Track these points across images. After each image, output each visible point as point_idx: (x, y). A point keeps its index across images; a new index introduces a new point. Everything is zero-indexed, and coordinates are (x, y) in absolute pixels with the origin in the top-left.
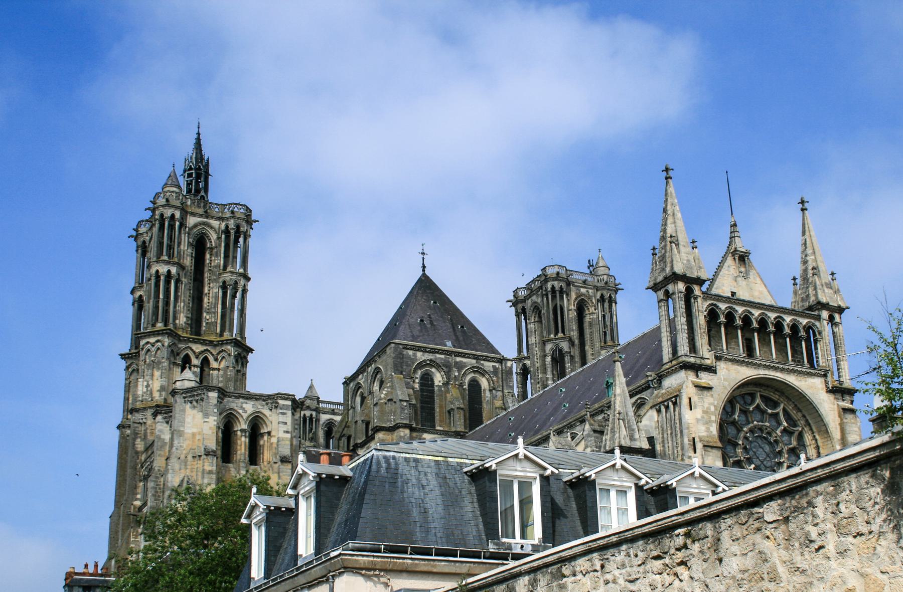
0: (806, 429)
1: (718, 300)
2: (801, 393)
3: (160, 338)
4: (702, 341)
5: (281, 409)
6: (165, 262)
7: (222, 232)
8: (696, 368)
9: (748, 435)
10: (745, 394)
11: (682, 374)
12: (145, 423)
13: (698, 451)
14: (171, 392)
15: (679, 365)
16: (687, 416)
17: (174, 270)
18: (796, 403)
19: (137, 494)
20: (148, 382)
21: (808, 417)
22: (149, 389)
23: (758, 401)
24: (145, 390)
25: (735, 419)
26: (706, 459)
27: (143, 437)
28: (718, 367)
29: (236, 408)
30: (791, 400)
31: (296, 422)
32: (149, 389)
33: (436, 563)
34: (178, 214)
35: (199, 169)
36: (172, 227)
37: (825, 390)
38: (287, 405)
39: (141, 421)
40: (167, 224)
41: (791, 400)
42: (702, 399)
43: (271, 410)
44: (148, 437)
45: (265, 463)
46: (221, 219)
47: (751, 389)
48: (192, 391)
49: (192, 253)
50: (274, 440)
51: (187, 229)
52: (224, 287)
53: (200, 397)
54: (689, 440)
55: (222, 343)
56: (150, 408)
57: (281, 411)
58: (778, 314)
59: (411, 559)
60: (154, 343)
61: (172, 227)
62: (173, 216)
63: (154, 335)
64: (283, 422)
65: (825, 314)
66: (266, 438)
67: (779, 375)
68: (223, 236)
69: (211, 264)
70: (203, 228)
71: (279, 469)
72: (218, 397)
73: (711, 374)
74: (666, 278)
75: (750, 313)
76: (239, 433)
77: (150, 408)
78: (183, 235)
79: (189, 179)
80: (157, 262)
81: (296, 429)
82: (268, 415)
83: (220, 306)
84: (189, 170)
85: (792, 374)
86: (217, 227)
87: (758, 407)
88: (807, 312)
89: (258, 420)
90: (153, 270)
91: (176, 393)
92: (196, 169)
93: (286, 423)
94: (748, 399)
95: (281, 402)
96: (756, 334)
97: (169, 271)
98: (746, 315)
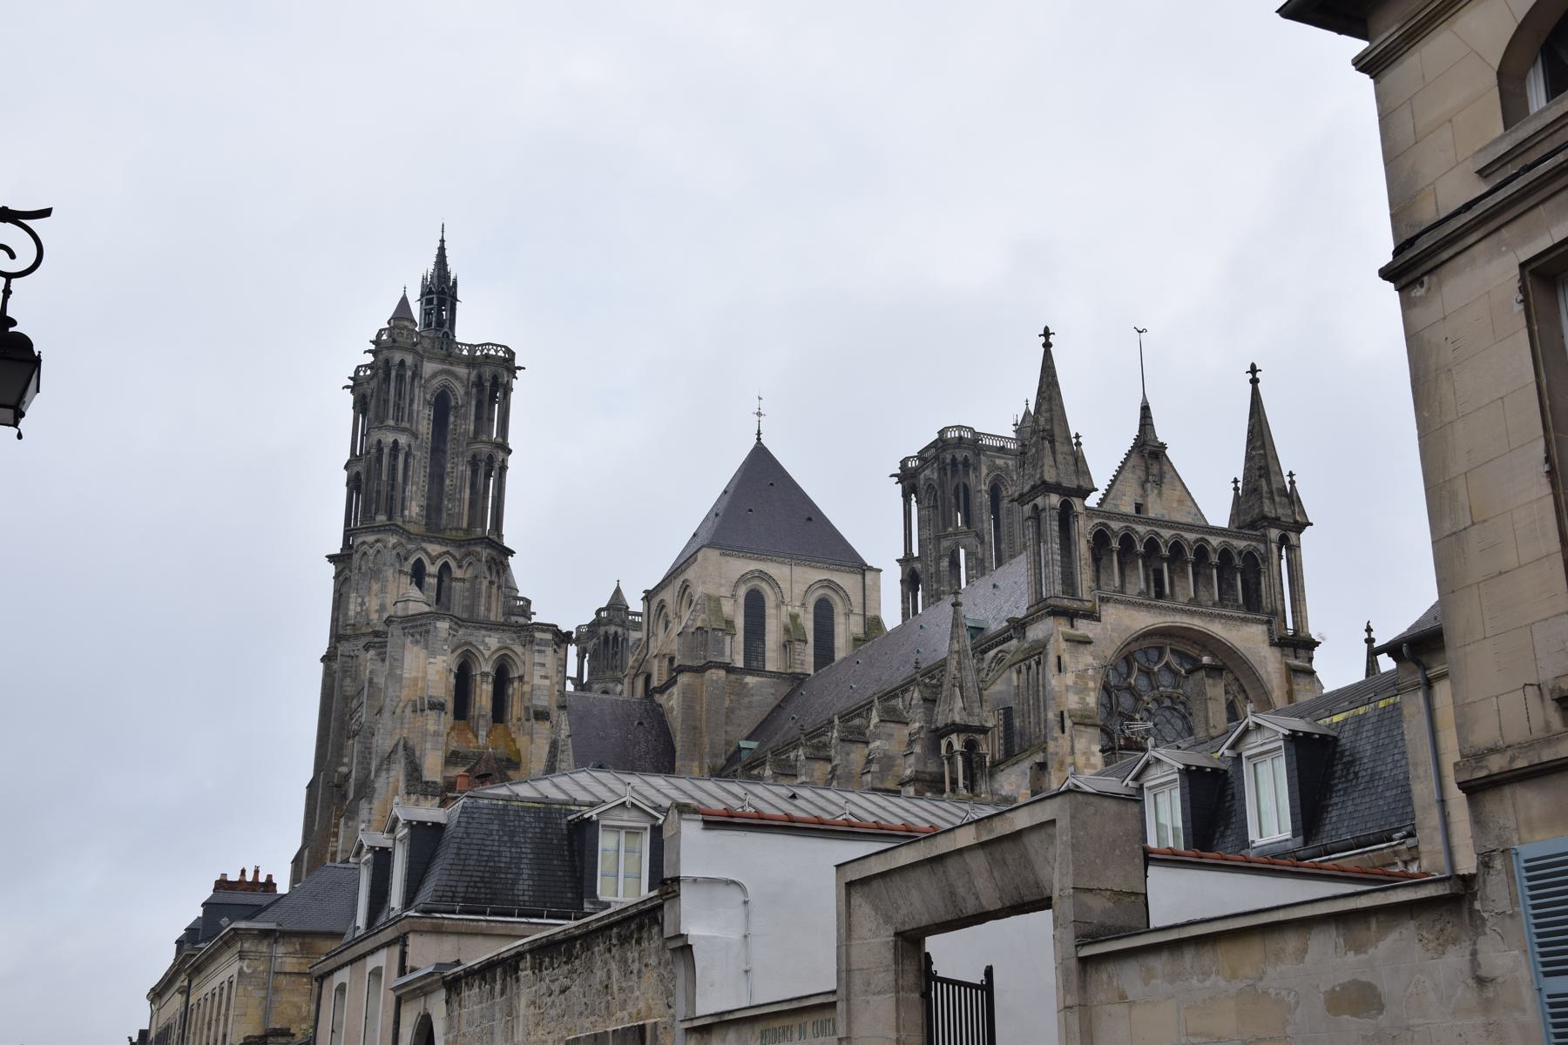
0: (1239, 697)
1: (1108, 518)
2: (1230, 648)
3: (379, 536)
4: (1084, 577)
5: (538, 644)
8: (1071, 615)
9: (1150, 706)
10: (1149, 648)
11: (1050, 622)
12: (357, 656)
13: (1067, 729)
14: (387, 620)
15: (1046, 611)
16: (1054, 682)
17: (403, 440)
18: (1224, 661)
20: (363, 598)
21: (1243, 682)
23: (1168, 657)
24: (359, 609)
25: (1130, 684)
26: (1076, 742)
27: (354, 676)
28: (1102, 613)
29: (474, 643)
30: (1218, 657)
31: (559, 662)
32: (364, 608)
33: (515, 925)
34: (409, 360)
35: (443, 292)
36: (400, 378)
37: (1268, 643)
38: (546, 640)
39: (352, 654)
40: (393, 374)
41: (1218, 657)
42: (1077, 658)
43: (524, 646)
45: (514, 720)
47: (1156, 641)
48: (414, 620)
49: (429, 415)
50: (527, 688)
51: (423, 381)
52: (474, 463)
53: (425, 628)
54: (1056, 716)
55: (469, 542)
57: (537, 648)
58: (1199, 536)
59: (486, 921)
60: (373, 543)
61: (400, 378)
62: (402, 363)
63: (373, 531)
64: (540, 664)
65: (1274, 534)
66: (516, 684)
67: (1197, 623)
68: (474, 390)
69: (455, 430)
71: (532, 729)
72: (450, 628)
73: (1093, 622)
74: (1033, 488)
75: (1157, 534)
76: (478, 678)
78: (417, 390)
79: (428, 307)
81: (560, 672)
82: (520, 654)
83: (468, 491)
84: (428, 293)
85: (1217, 621)
87: (1167, 665)
88: (1247, 532)
89: (505, 660)
91: (391, 621)
92: (438, 293)
93: (544, 665)
94: (1154, 654)
95: (538, 635)
96: (1165, 565)
97: (396, 442)
98: (1151, 538)
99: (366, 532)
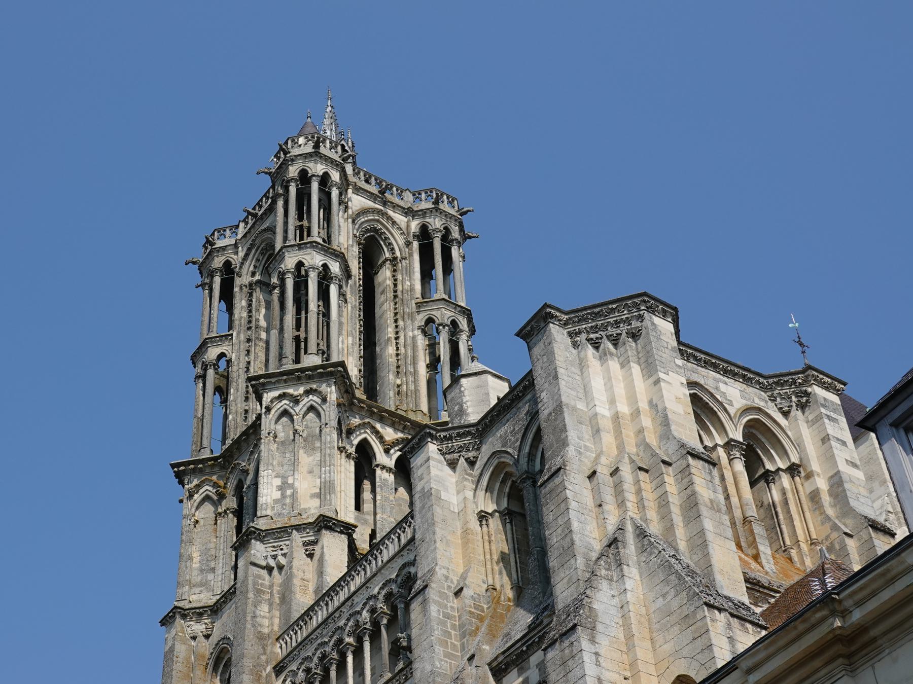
6: (314, 245)
7: (414, 237)
12: (281, 568)
22: (289, 492)
32: (289, 492)
34: (335, 176)
39: (272, 563)
44: (298, 596)
46: (409, 212)
56: (298, 528)
68: (416, 244)
70: (378, 221)
77: (298, 528)
80: (300, 247)
86: (403, 225)
90: (290, 262)
99: (285, 381)
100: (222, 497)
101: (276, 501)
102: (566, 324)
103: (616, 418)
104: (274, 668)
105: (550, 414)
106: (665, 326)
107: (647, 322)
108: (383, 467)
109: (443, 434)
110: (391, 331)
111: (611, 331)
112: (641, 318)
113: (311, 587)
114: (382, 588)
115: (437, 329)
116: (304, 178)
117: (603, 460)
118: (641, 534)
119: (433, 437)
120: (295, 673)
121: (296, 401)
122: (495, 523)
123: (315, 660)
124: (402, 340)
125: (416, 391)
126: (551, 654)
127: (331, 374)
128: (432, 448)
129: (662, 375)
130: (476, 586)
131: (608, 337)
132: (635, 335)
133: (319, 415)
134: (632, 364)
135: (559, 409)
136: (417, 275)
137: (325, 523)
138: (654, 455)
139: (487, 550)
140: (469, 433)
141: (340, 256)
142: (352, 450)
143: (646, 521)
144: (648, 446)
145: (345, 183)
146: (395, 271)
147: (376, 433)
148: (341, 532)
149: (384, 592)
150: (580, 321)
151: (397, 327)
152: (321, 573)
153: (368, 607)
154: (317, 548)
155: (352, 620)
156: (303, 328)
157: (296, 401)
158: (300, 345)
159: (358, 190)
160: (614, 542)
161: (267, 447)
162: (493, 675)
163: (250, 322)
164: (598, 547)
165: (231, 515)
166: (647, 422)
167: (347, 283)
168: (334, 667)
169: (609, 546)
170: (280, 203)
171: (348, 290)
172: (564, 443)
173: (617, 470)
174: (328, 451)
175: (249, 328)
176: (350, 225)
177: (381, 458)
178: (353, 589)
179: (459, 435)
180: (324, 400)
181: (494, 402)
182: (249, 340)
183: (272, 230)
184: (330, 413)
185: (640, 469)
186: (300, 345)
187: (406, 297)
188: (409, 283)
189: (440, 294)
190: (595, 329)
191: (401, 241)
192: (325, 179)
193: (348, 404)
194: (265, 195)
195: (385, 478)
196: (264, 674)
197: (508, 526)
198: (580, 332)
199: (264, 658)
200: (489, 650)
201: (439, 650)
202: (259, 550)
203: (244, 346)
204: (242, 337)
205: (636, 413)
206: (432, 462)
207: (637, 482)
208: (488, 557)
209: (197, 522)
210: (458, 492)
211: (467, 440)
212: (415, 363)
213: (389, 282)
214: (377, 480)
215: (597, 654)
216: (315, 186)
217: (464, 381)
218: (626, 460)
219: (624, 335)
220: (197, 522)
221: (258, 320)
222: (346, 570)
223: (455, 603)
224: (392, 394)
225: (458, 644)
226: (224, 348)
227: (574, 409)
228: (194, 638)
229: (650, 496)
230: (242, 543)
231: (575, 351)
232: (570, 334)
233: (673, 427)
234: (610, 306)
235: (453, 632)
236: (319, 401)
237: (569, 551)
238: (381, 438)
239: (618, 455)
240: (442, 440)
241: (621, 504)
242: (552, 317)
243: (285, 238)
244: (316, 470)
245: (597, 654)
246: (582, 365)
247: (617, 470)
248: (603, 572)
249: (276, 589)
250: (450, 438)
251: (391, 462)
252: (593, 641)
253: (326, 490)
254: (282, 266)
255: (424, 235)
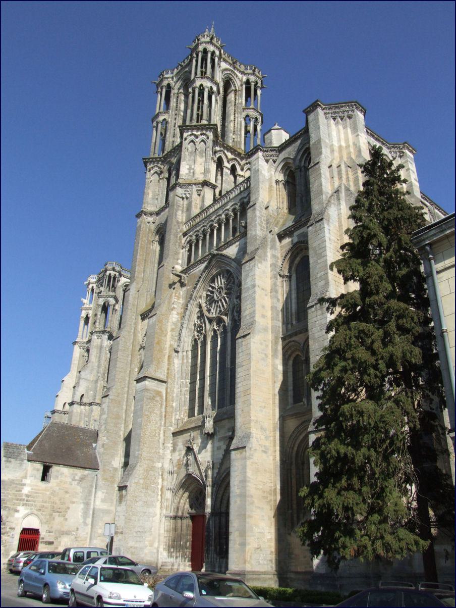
6: (208, 78)
12: (187, 198)
19: (178, 259)
22: (192, 171)
34: (217, 53)
39: (184, 196)
46: (243, 73)
56: (195, 184)
68: (244, 86)
77: (195, 184)
100: (162, 172)
101: (187, 174)
102: (324, 109)
103: (340, 147)
104: (183, 234)
105: (315, 142)
106: (361, 116)
107: (355, 113)
108: (226, 167)
109: (265, 149)
110: (232, 118)
111: (341, 114)
112: (353, 111)
113: (199, 206)
114: (231, 207)
115: (250, 119)
116: (205, 51)
117: (334, 161)
118: (347, 189)
119: (261, 150)
120: (191, 236)
121: (197, 137)
122: (281, 186)
123: (201, 232)
124: (236, 122)
125: (240, 141)
126: (310, 228)
127: (211, 129)
128: (260, 154)
129: (359, 133)
130: (273, 206)
131: (340, 117)
132: (350, 117)
133: (205, 144)
134: (348, 128)
135: (319, 141)
136: (244, 98)
137: (205, 183)
138: (354, 162)
139: (278, 194)
140: (275, 150)
141: (217, 84)
142: (216, 159)
143: (349, 185)
144: (352, 158)
145: (220, 57)
146: (236, 95)
147: (225, 155)
148: (212, 188)
149: (232, 208)
150: (329, 109)
151: (235, 116)
152: (203, 201)
153: (225, 213)
154: (202, 192)
155: (217, 218)
156: (200, 111)
157: (197, 137)
158: (199, 117)
159: (225, 60)
160: (337, 191)
161: (185, 154)
162: (279, 239)
163: (177, 108)
164: (330, 193)
165: (165, 179)
166: (352, 150)
167: (218, 95)
168: (208, 235)
169: (335, 193)
170: (194, 61)
171: (218, 98)
172: (321, 153)
173: (339, 166)
174: (208, 157)
175: (176, 110)
176: (221, 74)
177: (226, 164)
178: (208, 213)
179: (271, 150)
180: (208, 138)
181: (284, 141)
182: (176, 115)
183: (190, 72)
184: (210, 143)
185: (349, 166)
186: (199, 117)
187: (240, 106)
188: (240, 100)
189: (252, 106)
190: (335, 113)
191: (239, 84)
192: (213, 53)
193: (215, 143)
194: (187, 58)
195: (226, 171)
196: (179, 236)
197: (287, 186)
198: (329, 113)
199: (179, 230)
200: (276, 230)
201: (258, 228)
202: (179, 191)
203: (174, 117)
204: (173, 113)
205: (348, 147)
206: (260, 159)
207: (347, 171)
208: (278, 196)
209: (151, 181)
210: (268, 172)
211: (274, 153)
212: (240, 131)
213: (233, 99)
214: (224, 172)
215: (329, 230)
216: (209, 55)
217: (272, 131)
218: (343, 163)
219: (346, 116)
220: (151, 181)
221: (180, 107)
222: (212, 202)
223: (265, 211)
224: (231, 141)
225: (265, 226)
226: (166, 116)
227: (325, 142)
228: (149, 223)
229: (351, 177)
230: (170, 189)
231: (326, 121)
232: (325, 113)
233: (362, 153)
234: (342, 105)
235: (264, 222)
236: (206, 138)
237: (320, 192)
238: (227, 157)
239: (340, 161)
240: (264, 151)
241: (340, 178)
242: (319, 105)
243: (196, 74)
244: (203, 164)
245: (329, 230)
246: (328, 126)
247: (339, 166)
248: (333, 201)
249: (185, 206)
250: (268, 151)
251: (229, 166)
252: (328, 224)
253: (206, 172)
254: (194, 85)
255: (248, 83)
